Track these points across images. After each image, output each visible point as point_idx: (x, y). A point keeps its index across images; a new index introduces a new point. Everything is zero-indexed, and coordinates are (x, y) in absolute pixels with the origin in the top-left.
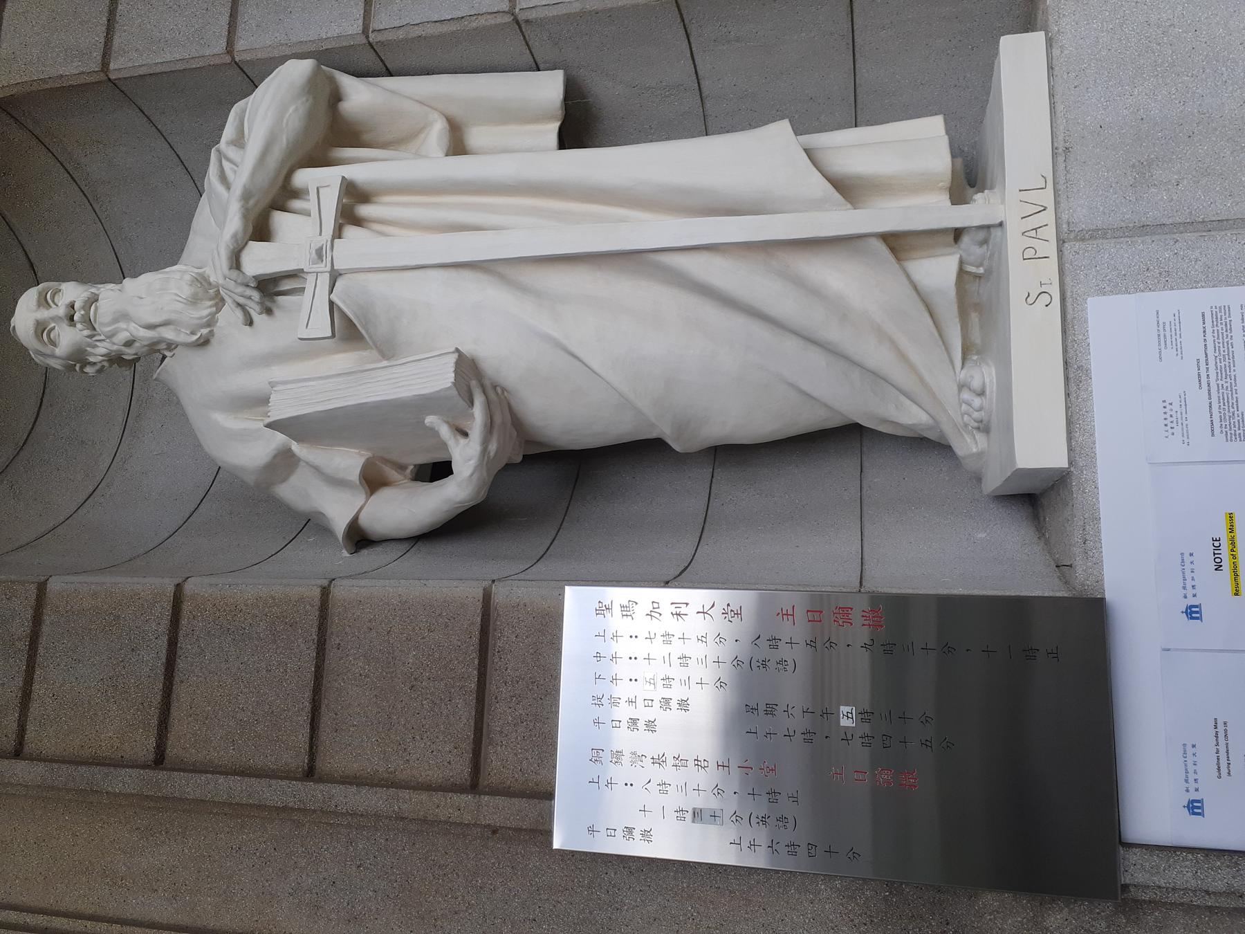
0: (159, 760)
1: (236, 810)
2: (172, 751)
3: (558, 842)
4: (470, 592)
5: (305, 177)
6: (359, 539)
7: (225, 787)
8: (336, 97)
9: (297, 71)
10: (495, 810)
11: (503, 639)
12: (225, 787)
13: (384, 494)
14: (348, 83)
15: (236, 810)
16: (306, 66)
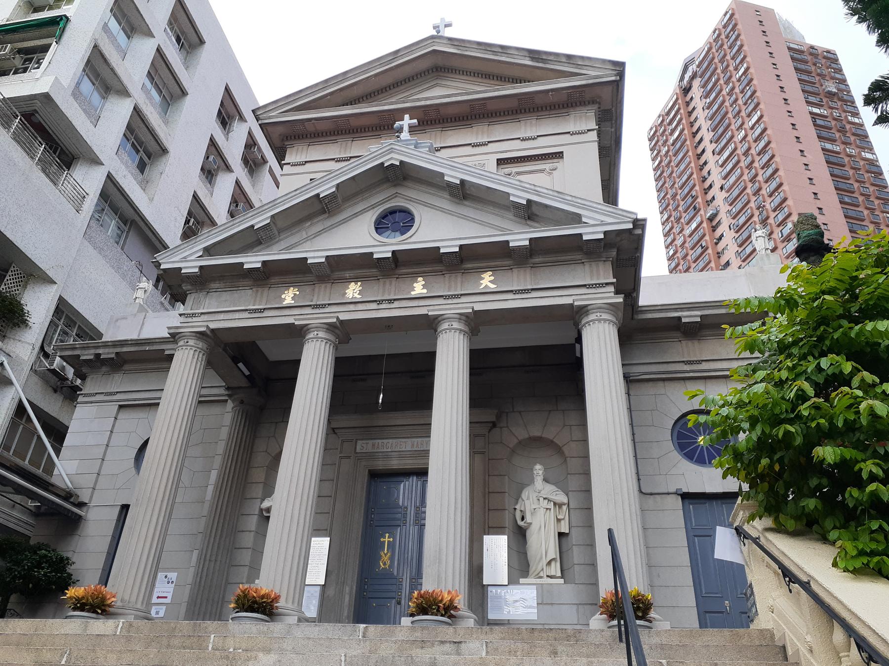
0: (489, 492)
1: (485, 502)
2: (490, 494)
3: (484, 536)
4: (507, 526)
5: (552, 503)
6: (515, 509)
7: (487, 501)
8: (564, 505)
9: (566, 501)
10: (487, 530)
11: (502, 529)
12: (487, 501)
13: (520, 512)
14: (566, 506)
15: (485, 502)
16: (566, 501)
